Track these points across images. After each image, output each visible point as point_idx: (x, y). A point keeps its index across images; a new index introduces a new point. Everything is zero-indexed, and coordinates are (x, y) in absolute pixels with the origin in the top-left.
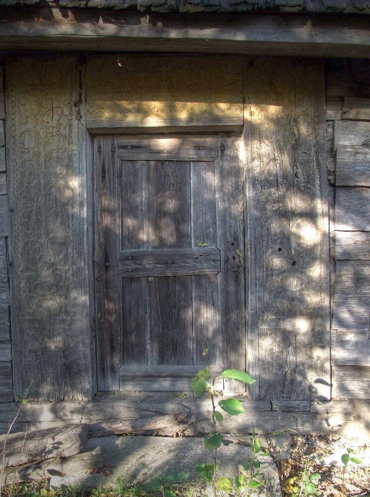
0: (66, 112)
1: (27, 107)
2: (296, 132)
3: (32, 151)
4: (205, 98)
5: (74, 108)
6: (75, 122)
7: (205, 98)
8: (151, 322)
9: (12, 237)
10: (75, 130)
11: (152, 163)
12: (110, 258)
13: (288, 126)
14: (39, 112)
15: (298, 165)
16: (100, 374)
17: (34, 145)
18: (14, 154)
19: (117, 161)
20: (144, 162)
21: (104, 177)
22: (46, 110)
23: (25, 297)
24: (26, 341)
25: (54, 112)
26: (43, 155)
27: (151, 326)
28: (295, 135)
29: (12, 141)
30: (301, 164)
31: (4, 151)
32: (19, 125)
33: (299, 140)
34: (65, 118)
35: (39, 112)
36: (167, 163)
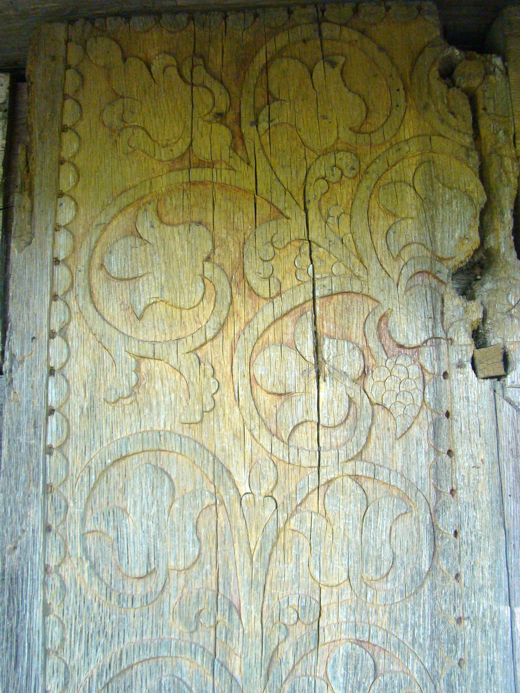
1: (147, 291)
5: (454, 303)
6: (469, 390)
14: (222, 326)
17: (193, 550)
22: (268, 312)
25: (326, 327)
26: (250, 619)
32: (90, 413)
34: (406, 368)
35: (222, 326)
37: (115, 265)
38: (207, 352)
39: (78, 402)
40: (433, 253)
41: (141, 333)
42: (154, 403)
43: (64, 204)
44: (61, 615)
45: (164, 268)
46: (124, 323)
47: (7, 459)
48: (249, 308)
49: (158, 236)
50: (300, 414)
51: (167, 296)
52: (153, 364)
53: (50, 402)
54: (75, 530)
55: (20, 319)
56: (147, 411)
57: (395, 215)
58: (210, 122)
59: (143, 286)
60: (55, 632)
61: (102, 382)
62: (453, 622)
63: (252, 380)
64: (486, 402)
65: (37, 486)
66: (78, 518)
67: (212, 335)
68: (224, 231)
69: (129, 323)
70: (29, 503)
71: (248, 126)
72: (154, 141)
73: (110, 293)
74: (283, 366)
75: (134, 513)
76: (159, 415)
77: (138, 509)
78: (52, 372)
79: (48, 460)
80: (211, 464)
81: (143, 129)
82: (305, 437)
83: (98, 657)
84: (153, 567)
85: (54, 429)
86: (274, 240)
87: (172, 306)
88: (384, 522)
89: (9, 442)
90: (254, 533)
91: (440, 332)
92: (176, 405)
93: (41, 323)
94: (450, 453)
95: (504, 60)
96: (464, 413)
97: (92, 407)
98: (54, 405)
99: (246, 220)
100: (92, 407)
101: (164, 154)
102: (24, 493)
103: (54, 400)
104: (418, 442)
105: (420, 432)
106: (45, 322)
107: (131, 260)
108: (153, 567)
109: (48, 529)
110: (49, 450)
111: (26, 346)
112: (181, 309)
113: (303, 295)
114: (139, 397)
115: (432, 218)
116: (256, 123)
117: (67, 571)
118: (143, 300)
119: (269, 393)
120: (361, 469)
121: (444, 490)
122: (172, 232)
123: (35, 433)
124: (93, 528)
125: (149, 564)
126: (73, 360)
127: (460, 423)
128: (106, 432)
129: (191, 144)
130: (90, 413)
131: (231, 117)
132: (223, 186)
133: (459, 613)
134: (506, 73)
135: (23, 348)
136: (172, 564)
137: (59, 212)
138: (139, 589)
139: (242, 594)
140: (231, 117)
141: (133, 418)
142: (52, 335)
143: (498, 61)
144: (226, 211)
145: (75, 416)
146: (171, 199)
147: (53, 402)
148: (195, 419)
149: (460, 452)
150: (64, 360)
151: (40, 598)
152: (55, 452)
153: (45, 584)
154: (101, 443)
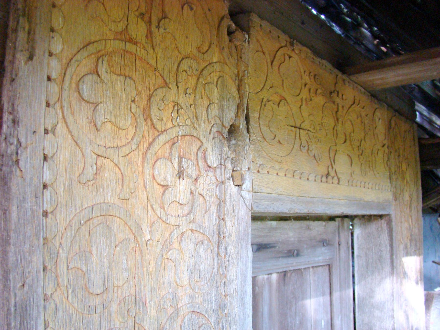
0: (213, 159)
32: (69, 189)
37: (86, 91)
38: (131, 158)
40: (222, 124)
41: (98, 140)
42: (105, 186)
43: (55, 38)
44: (54, 327)
45: (112, 101)
46: (89, 132)
47: (16, 220)
48: (151, 135)
49: (109, 79)
51: (113, 120)
52: (104, 161)
53: (44, 180)
54: (62, 269)
55: (25, 116)
56: (101, 190)
57: (210, 100)
58: (138, 17)
59: (101, 110)
61: (76, 169)
62: (223, 297)
65: (39, 240)
66: (65, 260)
67: (135, 148)
68: (141, 87)
69: (92, 132)
70: (33, 252)
71: (154, 27)
72: (109, 16)
73: (80, 110)
74: (166, 171)
75: (97, 254)
76: (108, 193)
77: (99, 253)
78: (45, 158)
79: (44, 221)
80: (134, 224)
81: (103, 4)
84: (106, 287)
85: (49, 199)
86: (164, 99)
87: (115, 126)
89: (18, 207)
90: (152, 262)
91: (223, 163)
92: (116, 188)
93: (40, 122)
94: (223, 219)
95: (249, 37)
96: (229, 201)
97: (70, 186)
98: (48, 182)
99: (151, 83)
100: (70, 186)
101: (113, 26)
102: (30, 245)
103: (48, 178)
104: (213, 213)
106: (42, 121)
107: (95, 90)
108: (106, 287)
109: (45, 269)
110: (45, 214)
111: (29, 137)
112: (119, 128)
114: (97, 180)
115: (223, 105)
116: (158, 27)
117: (57, 297)
118: (101, 119)
119: (159, 184)
121: (221, 236)
122: (117, 79)
123: (36, 201)
124: (73, 266)
125: (104, 285)
126: (59, 152)
128: (78, 202)
129: (127, 27)
130: (69, 189)
131: (146, 17)
132: (141, 59)
133: (226, 293)
135: (27, 138)
136: (116, 283)
137: (52, 42)
139: (147, 296)
140: (146, 17)
141: (94, 194)
142: (46, 132)
144: (142, 74)
145: (61, 190)
146: (115, 57)
147: (47, 180)
148: (127, 197)
149: (227, 219)
150: (55, 151)
151: (42, 318)
152: (50, 216)
153: (45, 307)
154: (76, 210)
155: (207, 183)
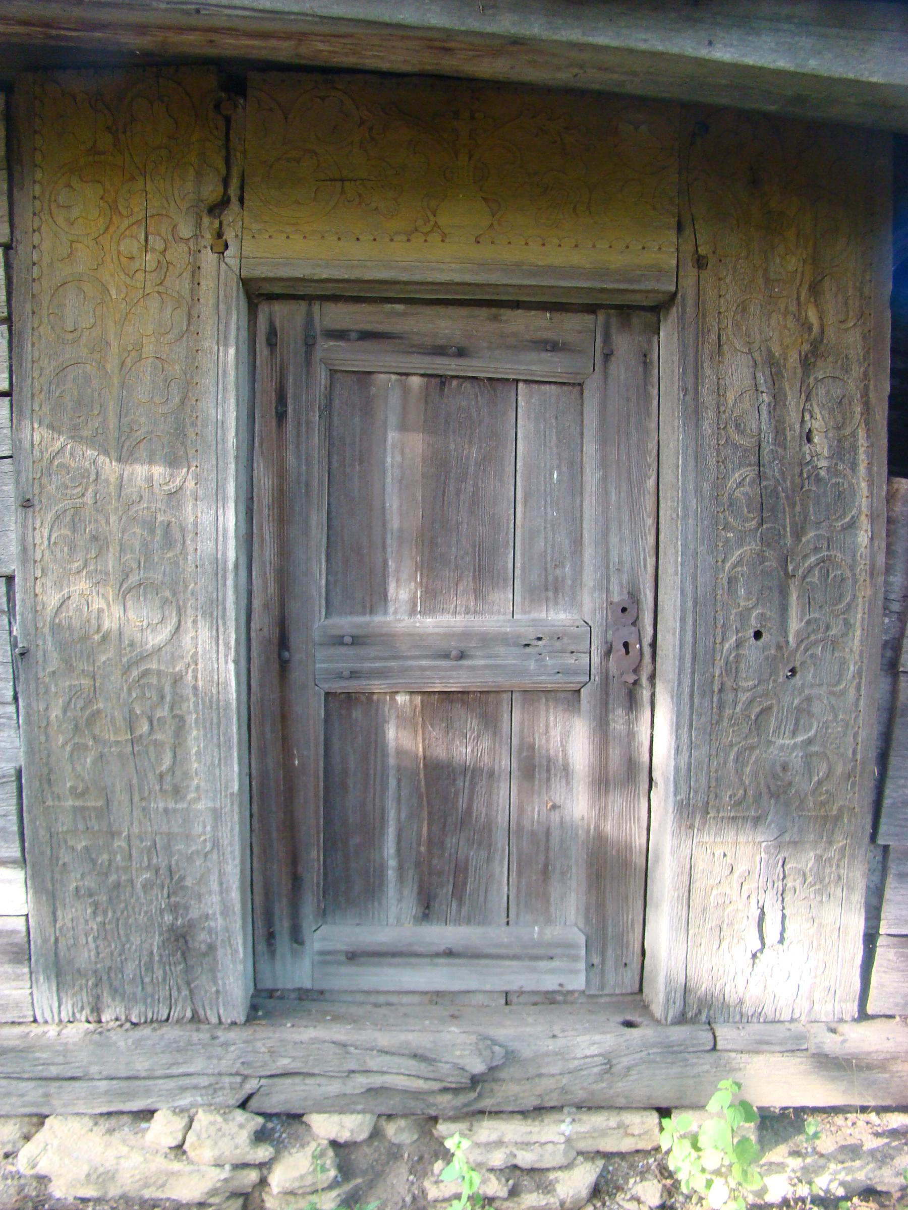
0: (186, 230)
1: (75, 212)
2: (813, 318)
3: (84, 340)
4: (574, 209)
5: (206, 220)
6: (209, 258)
7: (574, 209)
8: (399, 811)
9: (25, 580)
10: (207, 283)
11: (415, 382)
12: (292, 639)
13: (795, 302)
14: (107, 228)
15: (817, 410)
16: (262, 947)
17: (92, 321)
18: (33, 344)
19: (321, 376)
20: (394, 377)
21: (281, 417)
22: (126, 223)
23: (63, 746)
24: (64, 864)
25: (151, 229)
27: (399, 821)
28: (810, 329)
29: (28, 307)
30: (822, 406)
31: (6, 334)
33: (822, 341)
34: (183, 248)
35: (107, 228)
36: (455, 383)
37: (61, 199)
39: (46, 259)
50: (137, 266)
54: (45, 312)
60: (36, 354)
63: (119, 252)
64: (215, 263)
78: (34, 247)
82: (140, 276)
83: (53, 364)
88: (169, 311)
97: (52, 263)
100: (52, 263)
105: (187, 275)
109: (34, 313)
110: (34, 280)
113: (141, 216)
116: (125, 132)
120: (161, 289)
127: (203, 272)
134: (244, 108)
138: (70, 337)
142: (34, 231)
143: (241, 101)
145: (44, 265)
155: (179, 254)
